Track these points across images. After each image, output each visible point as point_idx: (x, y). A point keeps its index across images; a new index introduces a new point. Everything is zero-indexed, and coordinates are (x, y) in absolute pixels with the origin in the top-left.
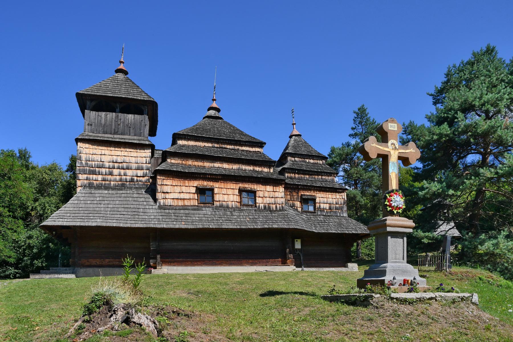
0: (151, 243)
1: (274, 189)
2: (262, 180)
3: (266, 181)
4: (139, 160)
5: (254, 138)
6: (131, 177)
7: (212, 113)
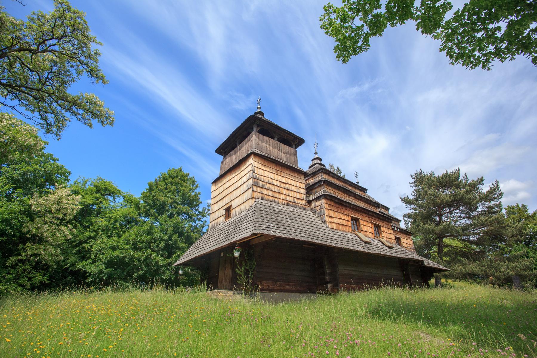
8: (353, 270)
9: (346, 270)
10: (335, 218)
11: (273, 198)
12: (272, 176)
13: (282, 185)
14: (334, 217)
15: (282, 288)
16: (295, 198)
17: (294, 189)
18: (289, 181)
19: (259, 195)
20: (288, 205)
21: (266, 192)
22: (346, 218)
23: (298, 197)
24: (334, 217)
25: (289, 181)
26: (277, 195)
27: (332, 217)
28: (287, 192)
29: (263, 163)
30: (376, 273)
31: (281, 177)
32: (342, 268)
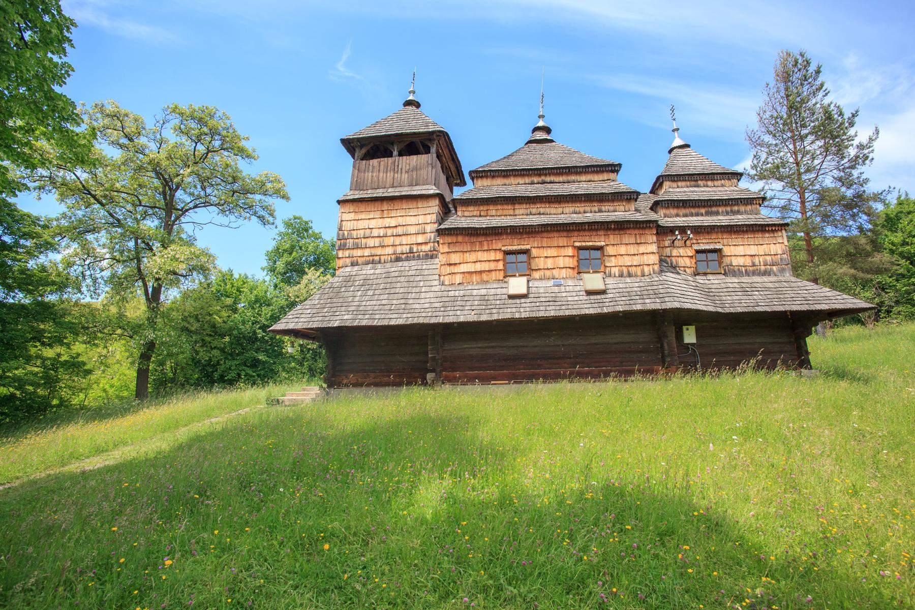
0: (429, 347)
1: (636, 239)
2: (613, 226)
3: (621, 227)
4: (421, 219)
5: (571, 153)
6: (409, 246)
7: (540, 135)
8: (492, 347)
9: (474, 348)
10: (462, 265)
11: (371, 258)
12: (373, 223)
13: (389, 232)
14: (460, 263)
15: (377, 380)
16: (413, 244)
17: (412, 230)
18: (401, 221)
19: (348, 261)
20: (398, 259)
21: (359, 253)
22: (492, 256)
23: (419, 241)
24: (460, 263)
25: (401, 221)
26: (379, 251)
27: (455, 264)
28: (398, 240)
29: (357, 209)
30: (559, 345)
31: (389, 220)
32: (466, 346)
